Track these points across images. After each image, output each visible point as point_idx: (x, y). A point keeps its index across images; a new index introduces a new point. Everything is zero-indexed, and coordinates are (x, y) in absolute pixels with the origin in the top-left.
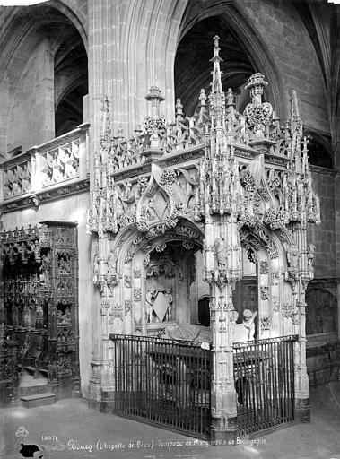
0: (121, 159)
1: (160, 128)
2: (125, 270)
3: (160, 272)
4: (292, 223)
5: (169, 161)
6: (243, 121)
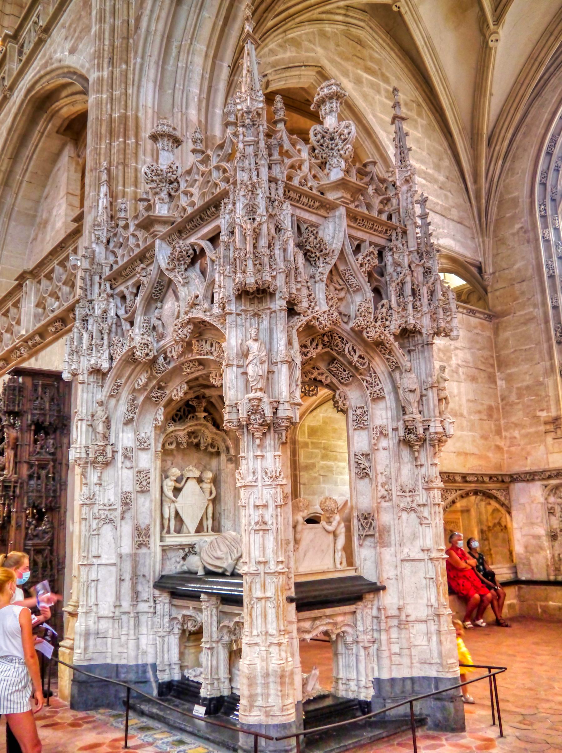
0: (120, 252)
1: (171, 183)
2: (125, 438)
3: (190, 444)
4: (406, 334)
5: (181, 230)
6: (305, 155)
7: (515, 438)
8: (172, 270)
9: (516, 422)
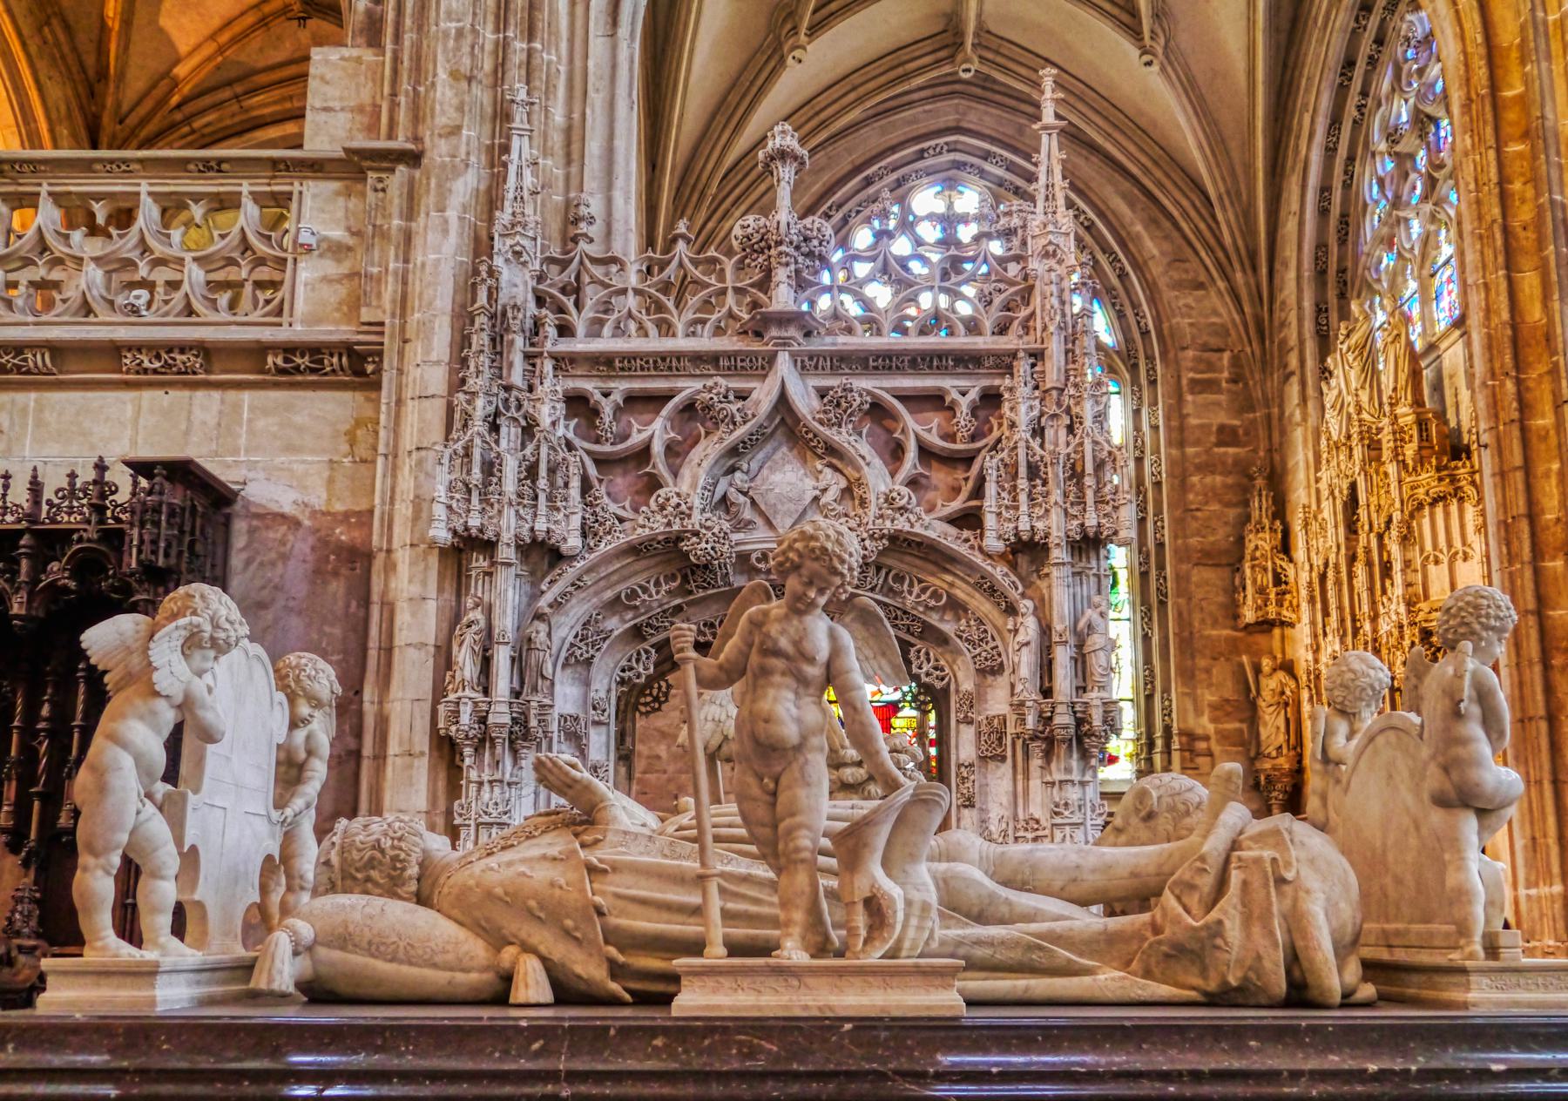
7: (658, 757)
8: (830, 425)
9: (665, 729)
